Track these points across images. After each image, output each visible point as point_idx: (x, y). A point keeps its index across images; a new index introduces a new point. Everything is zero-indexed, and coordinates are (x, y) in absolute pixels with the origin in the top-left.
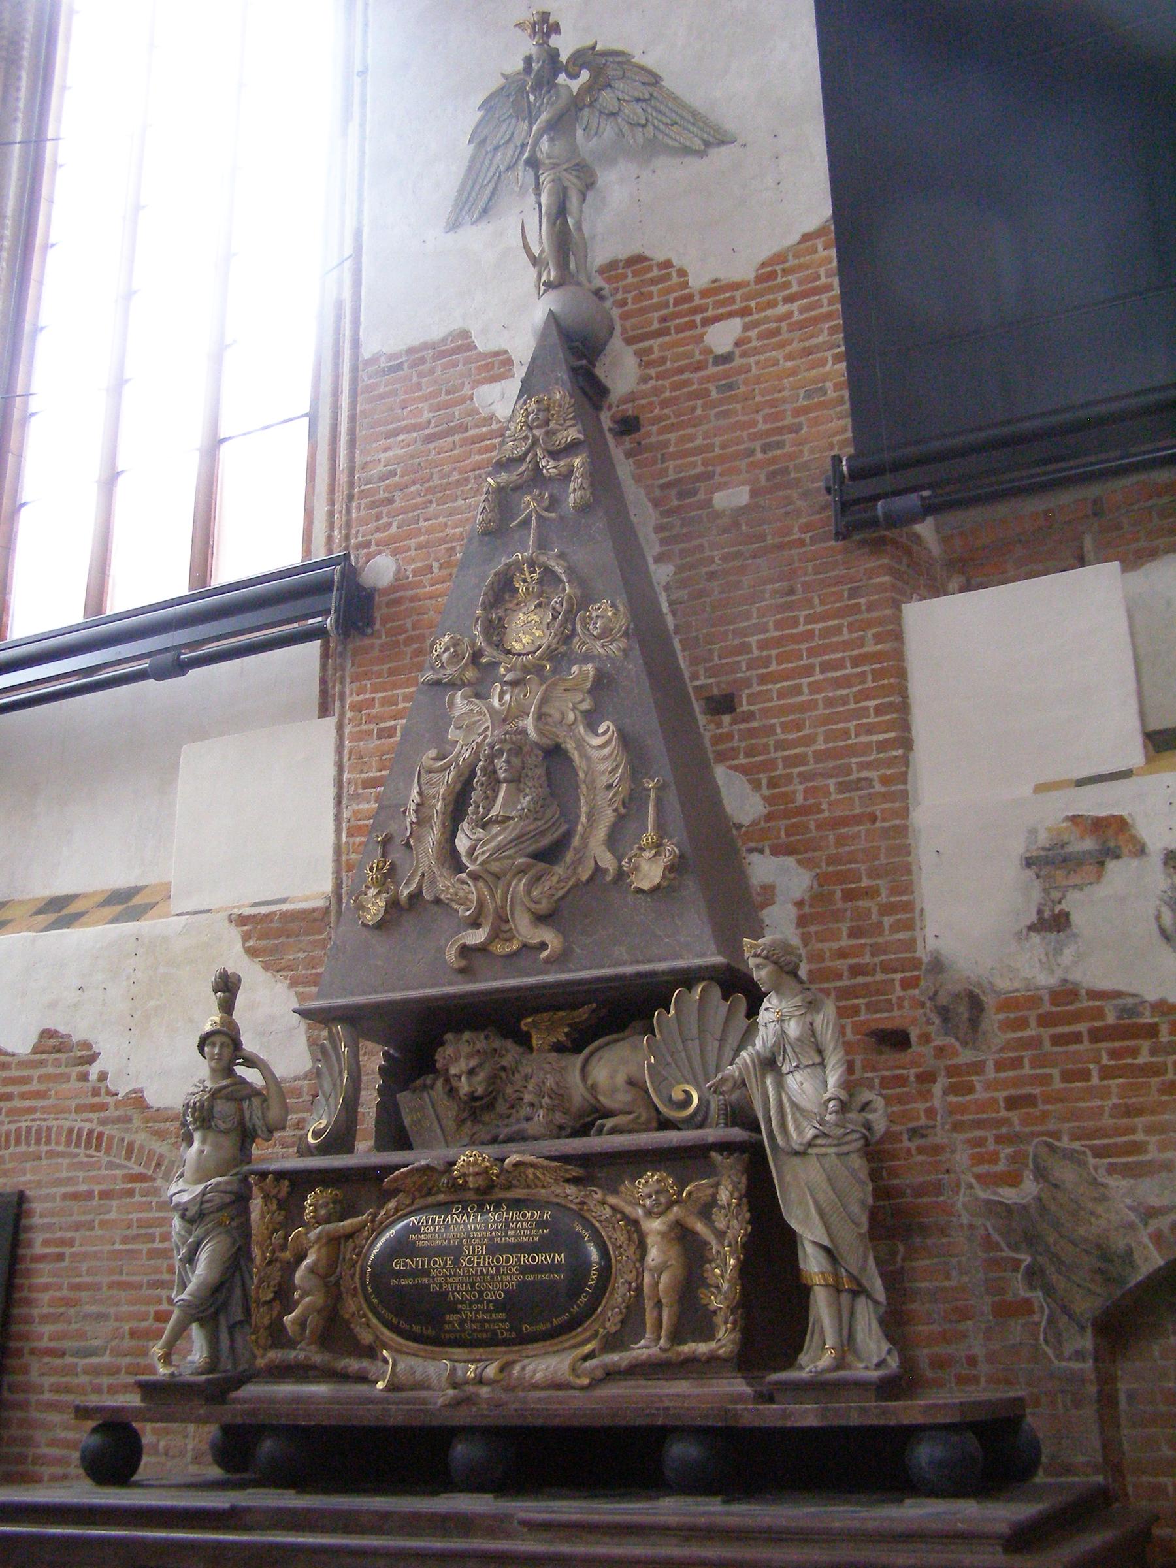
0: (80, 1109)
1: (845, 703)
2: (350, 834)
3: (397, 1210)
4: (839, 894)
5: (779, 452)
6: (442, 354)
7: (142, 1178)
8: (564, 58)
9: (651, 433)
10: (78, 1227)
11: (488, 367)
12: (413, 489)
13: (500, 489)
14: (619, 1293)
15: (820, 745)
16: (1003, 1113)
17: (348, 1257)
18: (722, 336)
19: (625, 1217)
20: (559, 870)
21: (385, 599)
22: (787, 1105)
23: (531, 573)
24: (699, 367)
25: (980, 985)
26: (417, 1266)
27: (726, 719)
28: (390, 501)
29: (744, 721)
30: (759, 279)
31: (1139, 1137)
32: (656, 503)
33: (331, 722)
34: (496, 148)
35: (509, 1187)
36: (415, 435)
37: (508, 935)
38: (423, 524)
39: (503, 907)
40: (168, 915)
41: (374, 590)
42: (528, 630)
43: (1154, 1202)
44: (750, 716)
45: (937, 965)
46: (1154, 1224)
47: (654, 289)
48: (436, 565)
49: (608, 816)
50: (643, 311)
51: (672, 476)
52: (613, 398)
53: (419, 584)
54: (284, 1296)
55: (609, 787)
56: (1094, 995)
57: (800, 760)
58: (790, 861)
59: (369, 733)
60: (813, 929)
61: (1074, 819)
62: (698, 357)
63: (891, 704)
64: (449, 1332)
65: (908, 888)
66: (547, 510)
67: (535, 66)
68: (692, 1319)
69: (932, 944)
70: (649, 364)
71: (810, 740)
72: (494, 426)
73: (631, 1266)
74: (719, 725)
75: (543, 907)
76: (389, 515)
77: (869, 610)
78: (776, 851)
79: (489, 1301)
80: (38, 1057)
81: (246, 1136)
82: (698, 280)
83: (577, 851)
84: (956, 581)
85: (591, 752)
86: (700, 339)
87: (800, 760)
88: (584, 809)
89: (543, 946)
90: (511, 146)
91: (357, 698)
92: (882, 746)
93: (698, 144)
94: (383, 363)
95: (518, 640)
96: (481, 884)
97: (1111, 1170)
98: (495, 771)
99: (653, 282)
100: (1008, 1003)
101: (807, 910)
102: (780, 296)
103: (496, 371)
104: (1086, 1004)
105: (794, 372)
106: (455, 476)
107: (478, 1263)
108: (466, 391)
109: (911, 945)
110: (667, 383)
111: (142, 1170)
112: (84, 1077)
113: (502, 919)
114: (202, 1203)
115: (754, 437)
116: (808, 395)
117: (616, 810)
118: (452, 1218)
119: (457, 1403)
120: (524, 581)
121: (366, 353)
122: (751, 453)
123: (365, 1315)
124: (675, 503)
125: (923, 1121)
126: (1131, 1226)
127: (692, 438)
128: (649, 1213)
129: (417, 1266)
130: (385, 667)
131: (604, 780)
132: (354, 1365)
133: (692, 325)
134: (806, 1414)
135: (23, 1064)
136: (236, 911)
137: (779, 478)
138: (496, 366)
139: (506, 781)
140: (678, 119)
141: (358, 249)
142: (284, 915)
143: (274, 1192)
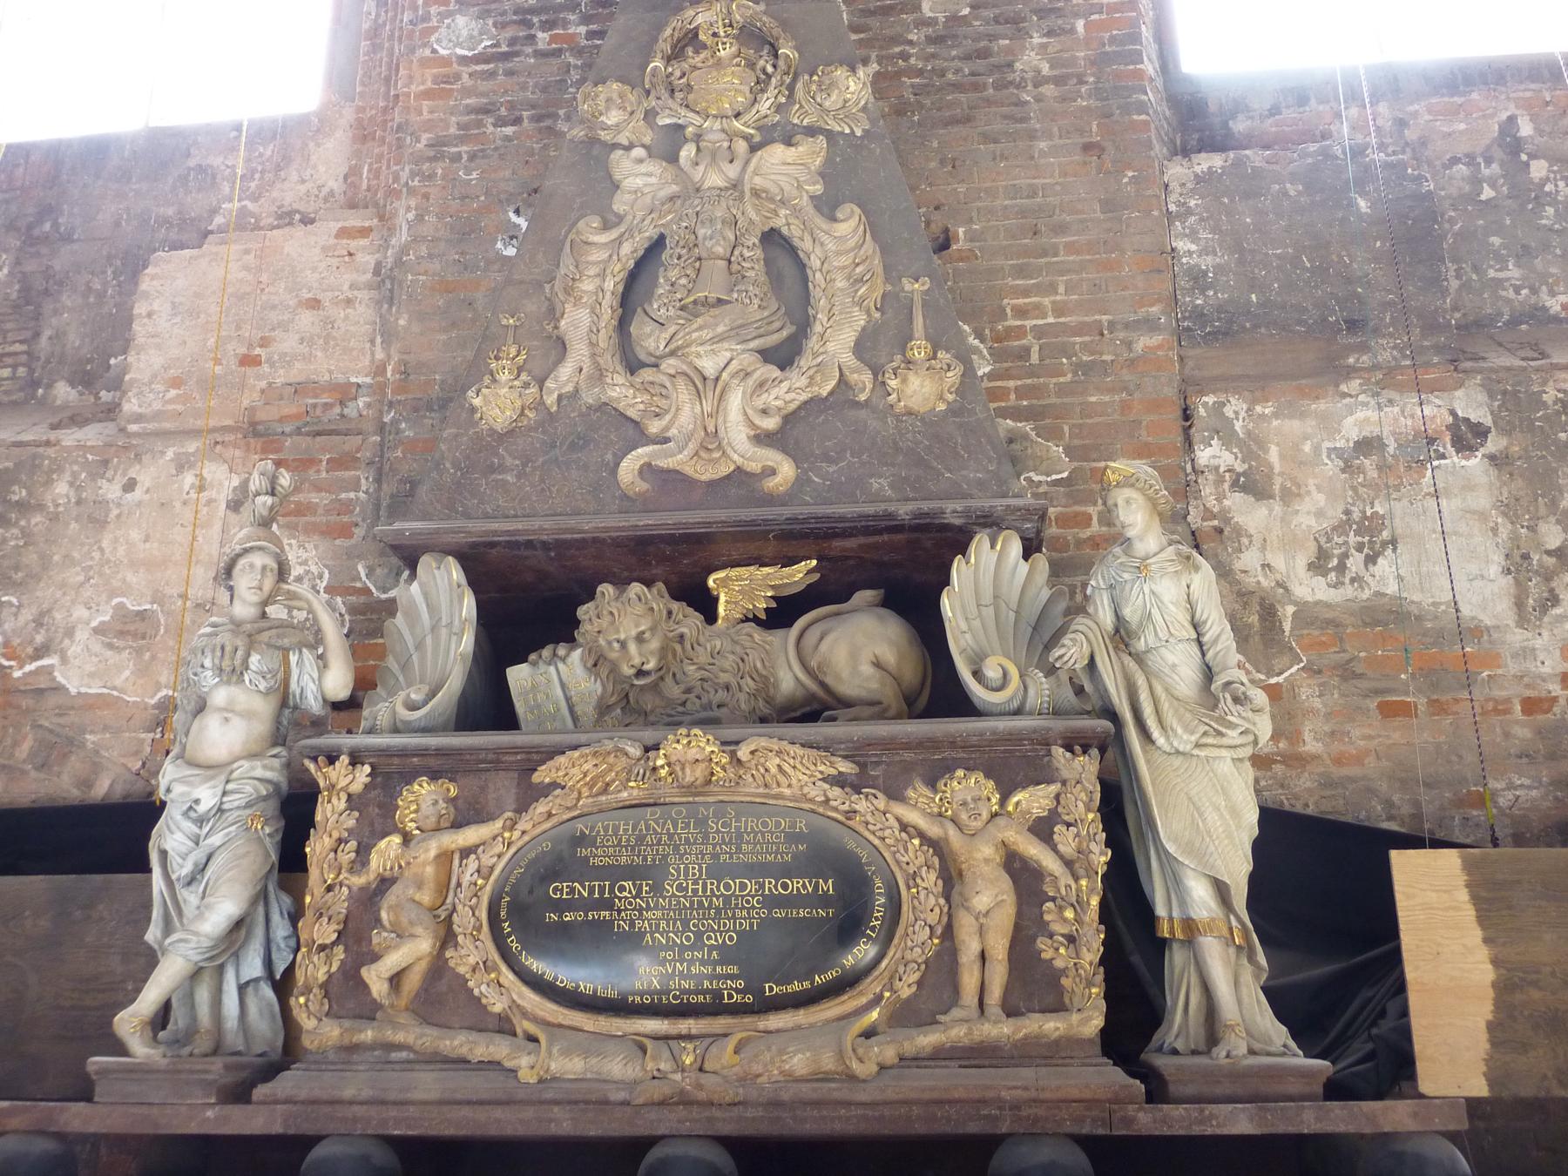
3: (550, 815)
17: (466, 879)
19: (921, 835)
26: (591, 892)
68: (1033, 984)
73: (932, 900)
75: (771, 423)
79: (712, 948)
107: (695, 891)
114: (224, 793)
117: (868, 312)
118: (648, 827)
123: (496, 969)
129: (591, 892)
143: (342, 783)
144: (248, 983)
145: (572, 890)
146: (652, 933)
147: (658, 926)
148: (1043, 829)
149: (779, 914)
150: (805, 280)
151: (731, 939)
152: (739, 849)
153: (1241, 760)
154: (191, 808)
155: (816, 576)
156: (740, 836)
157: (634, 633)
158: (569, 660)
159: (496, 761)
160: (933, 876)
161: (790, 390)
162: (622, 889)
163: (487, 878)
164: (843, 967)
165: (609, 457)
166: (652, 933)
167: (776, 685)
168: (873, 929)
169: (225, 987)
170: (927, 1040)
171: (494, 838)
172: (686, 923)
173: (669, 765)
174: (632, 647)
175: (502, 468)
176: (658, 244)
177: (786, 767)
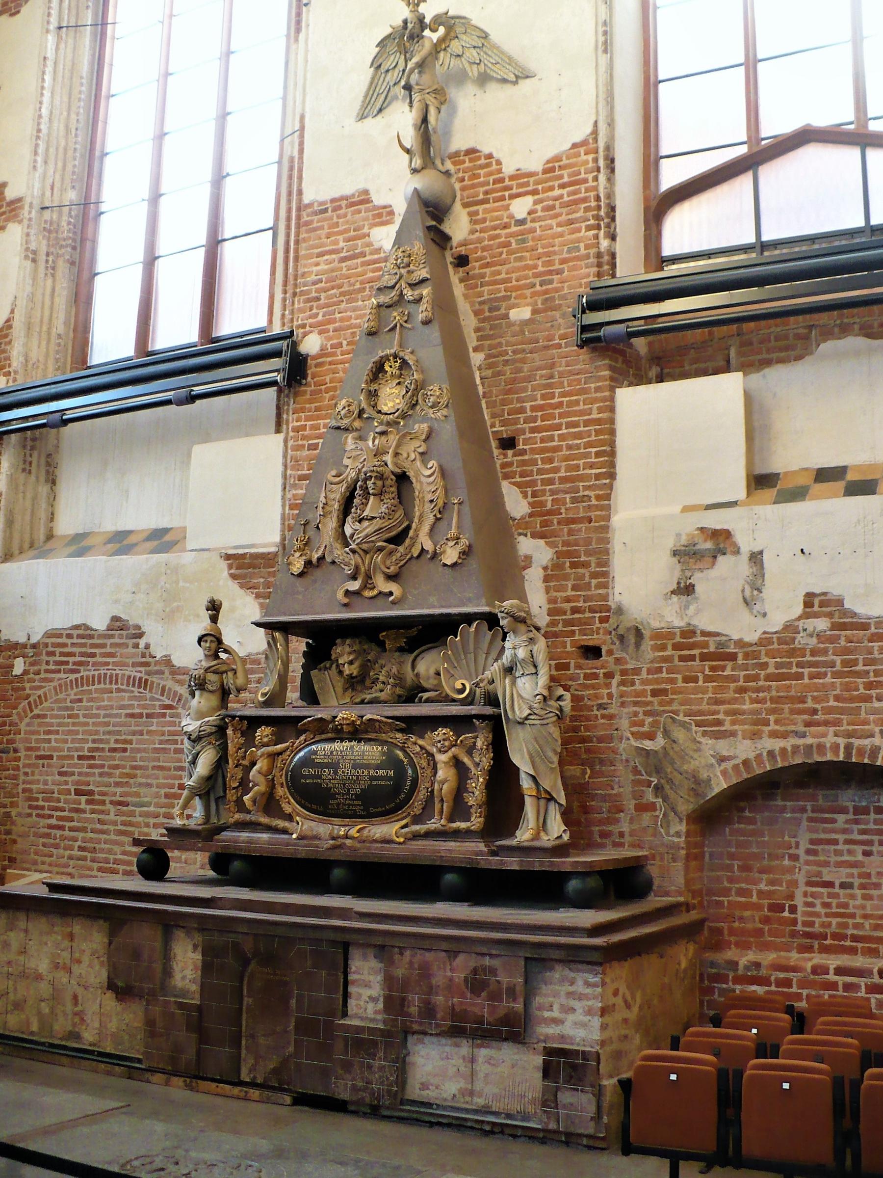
0: (134, 665)
1: (579, 449)
2: (291, 508)
4: (568, 564)
5: (550, 286)
6: (353, 204)
7: (170, 707)
8: (427, 20)
9: (475, 267)
10: (134, 733)
11: (380, 215)
12: (332, 292)
13: (379, 306)
14: (422, 794)
15: (562, 474)
16: (650, 698)
18: (520, 207)
19: (428, 753)
20: (401, 549)
21: (314, 362)
22: (515, 696)
24: (506, 226)
25: (642, 623)
27: (510, 453)
28: (318, 299)
29: (520, 455)
30: (545, 171)
31: (721, 716)
32: (476, 313)
33: (281, 437)
34: (388, 71)
35: (367, 732)
36: (334, 256)
38: (338, 316)
39: (369, 570)
40: (184, 550)
41: (307, 355)
42: (391, 398)
43: (725, 753)
44: (523, 453)
45: (620, 611)
46: (724, 765)
47: (482, 172)
48: (345, 343)
49: (430, 519)
50: (473, 186)
52: (455, 242)
53: (334, 354)
54: (244, 785)
55: (432, 501)
56: (704, 633)
57: (551, 482)
58: (542, 542)
59: (303, 446)
60: (552, 584)
61: (702, 529)
62: (506, 220)
63: (605, 451)
65: (606, 564)
67: (410, 26)
68: (459, 809)
69: (617, 598)
70: (476, 222)
71: (556, 470)
72: (382, 255)
74: (505, 456)
75: (393, 570)
76: (317, 308)
77: (596, 392)
78: (533, 536)
80: (110, 632)
81: (224, 693)
82: (508, 169)
84: (654, 372)
86: (507, 208)
87: (551, 482)
88: (417, 514)
89: (391, 594)
90: (397, 70)
92: (598, 477)
93: (512, 78)
94: (316, 207)
95: (386, 405)
97: (705, 734)
99: (481, 167)
100: (658, 635)
101: (549, 572)
102: (556, 183)
103: (384, 219)
104: (699, 638)
105: (561, 235)
106: (358, 286)
108: (366, 230)
109: (605, 598)
110: (486, 235)
111: (170, 702)
112: (136, 646)
113: (368, 577)
115: (536, 276)
116: (569, 251)
119: (334, 847)
121: (306, 200)
122: (534, 285)
124: (487, 314)
125: (605, 700)
126: (712, 765)
127: (499, 273)
128: (440, 751)
130: (313, 406)
131: (430, 497)
133: (503, 198)
134: (513, 863)
135: (100, 636)
137: (549, 306)
138: (383, 215)
139: (374, 495)
141: (302, 128)
148: (470, 751)
149: (374, 783)
175: (298, 593)
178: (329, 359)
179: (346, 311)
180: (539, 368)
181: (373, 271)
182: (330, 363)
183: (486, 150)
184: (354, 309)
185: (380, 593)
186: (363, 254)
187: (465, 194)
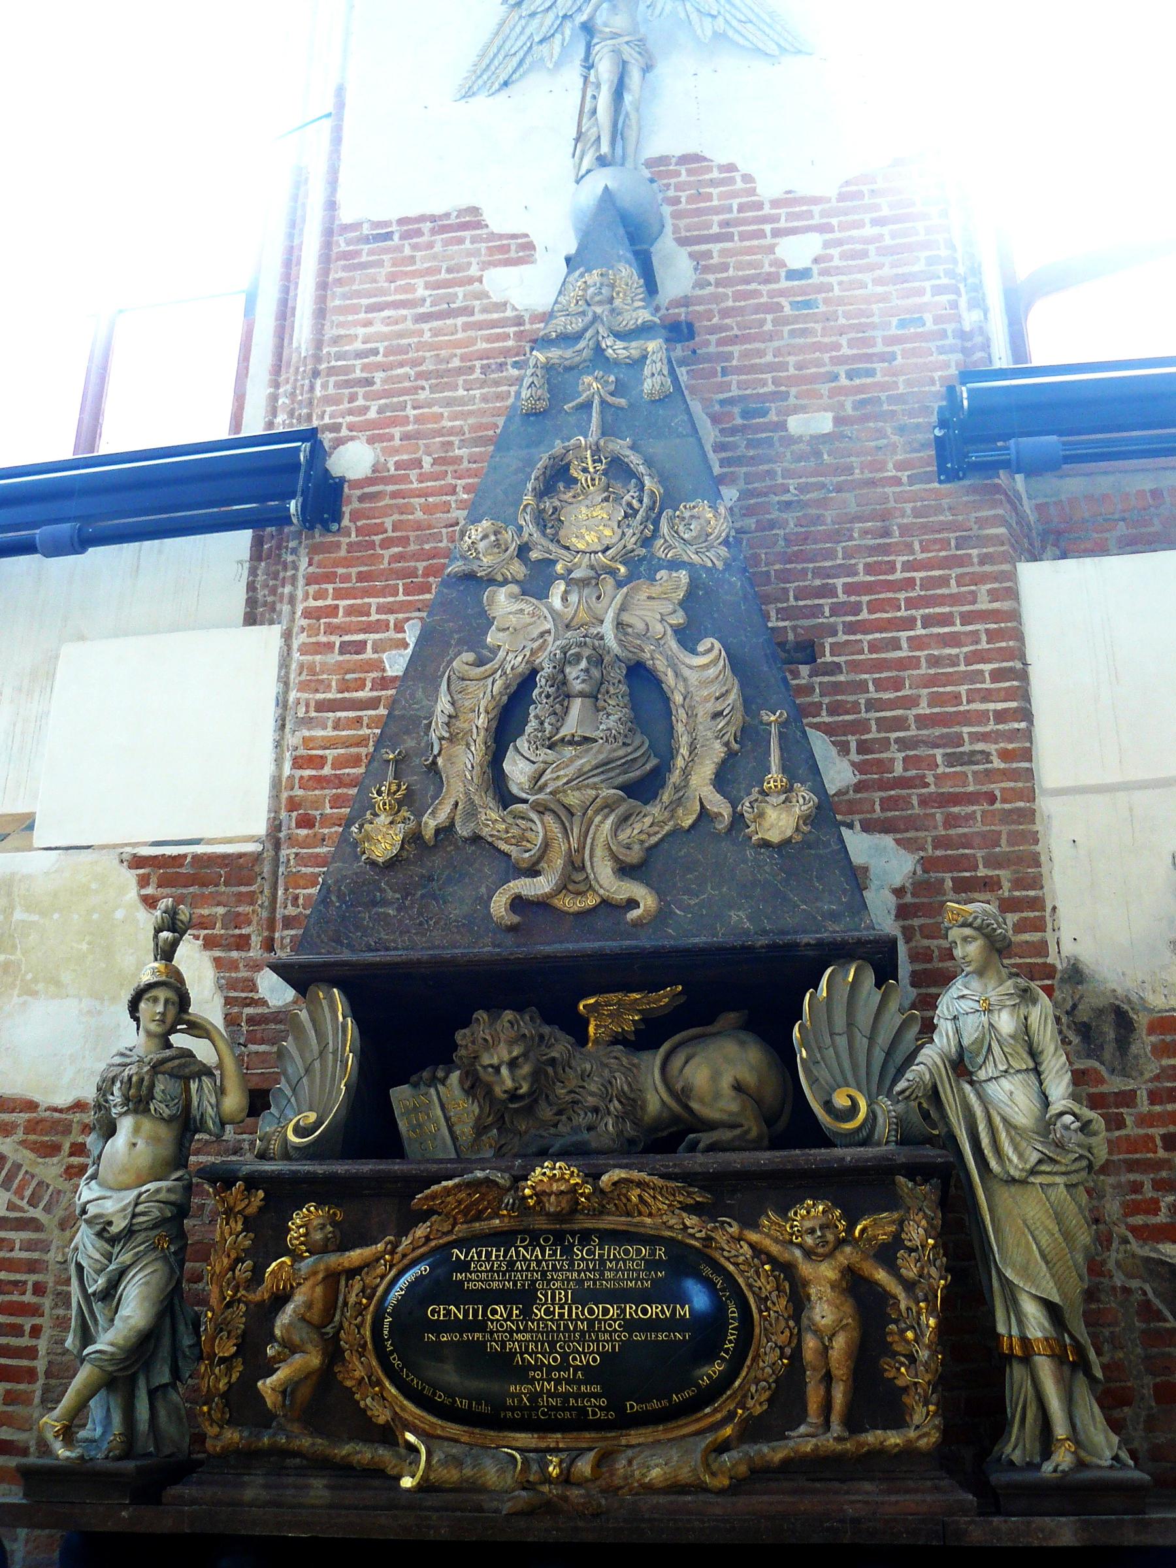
1: (955, 664)
2: (298, 763)
3: (428, 1239)
4: (949, 884)
5: (869, 380)
11: (505, 249)
12: (400, 371)
15: (924, 709)
16: (1161, 1154)
17: (352, 1299)
19: (772, 1259)
20: (655, 810)
21: (358, 492)
23: (594, 461)
24: (769, 279)
25: (1129, 1002)
28: (369, 382)
29: (825, 674)
30: (842, 197)
32: (715, 419)
33: (269, 637)
34: (533, 15)
35: (602, 1212)
36: (404, 312)
37: (582, 888)
38: (412, 413)
39: (581, 849)
40: (30, 848)
41: (342, 480)
44: (836, 668)
45: (1076, 974)
47: (715, 191)
51: (735, 392)
53: (405, 479)
54: (253, 1354)
55: (717, 715)
57: (899, 724)
58: (888, 840)
59: (329, 646)
60: (916, 922)
62: (767, 268)
63: (1011, 669)
64: (513, 1409)
65: (1036, 882)
66: (612, 394)
68: (875, 1399)
69: (1068, 948)
70: (707, 269)
71: (912, 702)
72: (509, 313)
73: (783, 1324)
75: (634, 856)
76: (366, 397)
77: (982, 563)
78: (867, 827)
83: (677, 789)
85: (686, 672)
86: (771, 249)
87: (899, 724)
88: (684, 740)
89: (632, 904)
90: (551, 15)
91: (312, 603)
92: (1000, 716)
93: (772, 48)
94: (366, 230)
95: (580, 537)
96: (549, 818)
98: (564, 682)
99: (713, 183)
101: (908, 899)
102: (867, 217)
103: (513, 254)
106: (456, 363)
107: (561, 1315)
108: (474, 271)
109: (1041, 948)
110: (729, 291)
113: (575, 866)
114: (134, 1216)
115: (836, 361)
116: (902, 324)
117: (727, 744)
118: (517, 1253)
119: (529, 1513)
120: (585, 470)
123: (379, 1383)
124: (739, 421)
130: (354, 571)
131: (711, 707)
132: (363, 1453)
133: (761, 234)
136: (128, 849)
139: (582, 694)
140: (753, 17)
141: (340, 105)
142: (196, 858)
144: (157, 1388)
145: (448, 1312)
146: (522, 1354)
147: (527, 1347)
148: (887, 1254)
149: (639, 1337)
150: (670, 713)
151: (594, 1360)
152: (602, 1274)
153: (1075, 1186)
154: (104, 1229)
155: (683, 999)
156: (602, 1262)
157: (506, 1057)
158: (448, 1082)
159: (377, 1186)
160: (783, 1302)
161: (649, 823)
162: (494, 1312)
163: (370, 1298)
164: (698, 1386)
165: (483, 890)
166: (522, 1354)
167: (643, 1108)
168: (727, 1351)
169: (137, 1393)
170: (774, 1453)
171: (377, 1260)
172: (552, 1345)
173: (536, 1194)
174: (504, 1071)
175: (385, 903)
176: (528, 680)
177: (646, 1196)
178: (390, 488)
179: (430, 406)
180: (859, 518)
181: (489, 339)
182: (394, 495)
183: (721, 157)
184: (449, 403)
185: (605, 902)
186: (468, 311)
187: (682, 223)
